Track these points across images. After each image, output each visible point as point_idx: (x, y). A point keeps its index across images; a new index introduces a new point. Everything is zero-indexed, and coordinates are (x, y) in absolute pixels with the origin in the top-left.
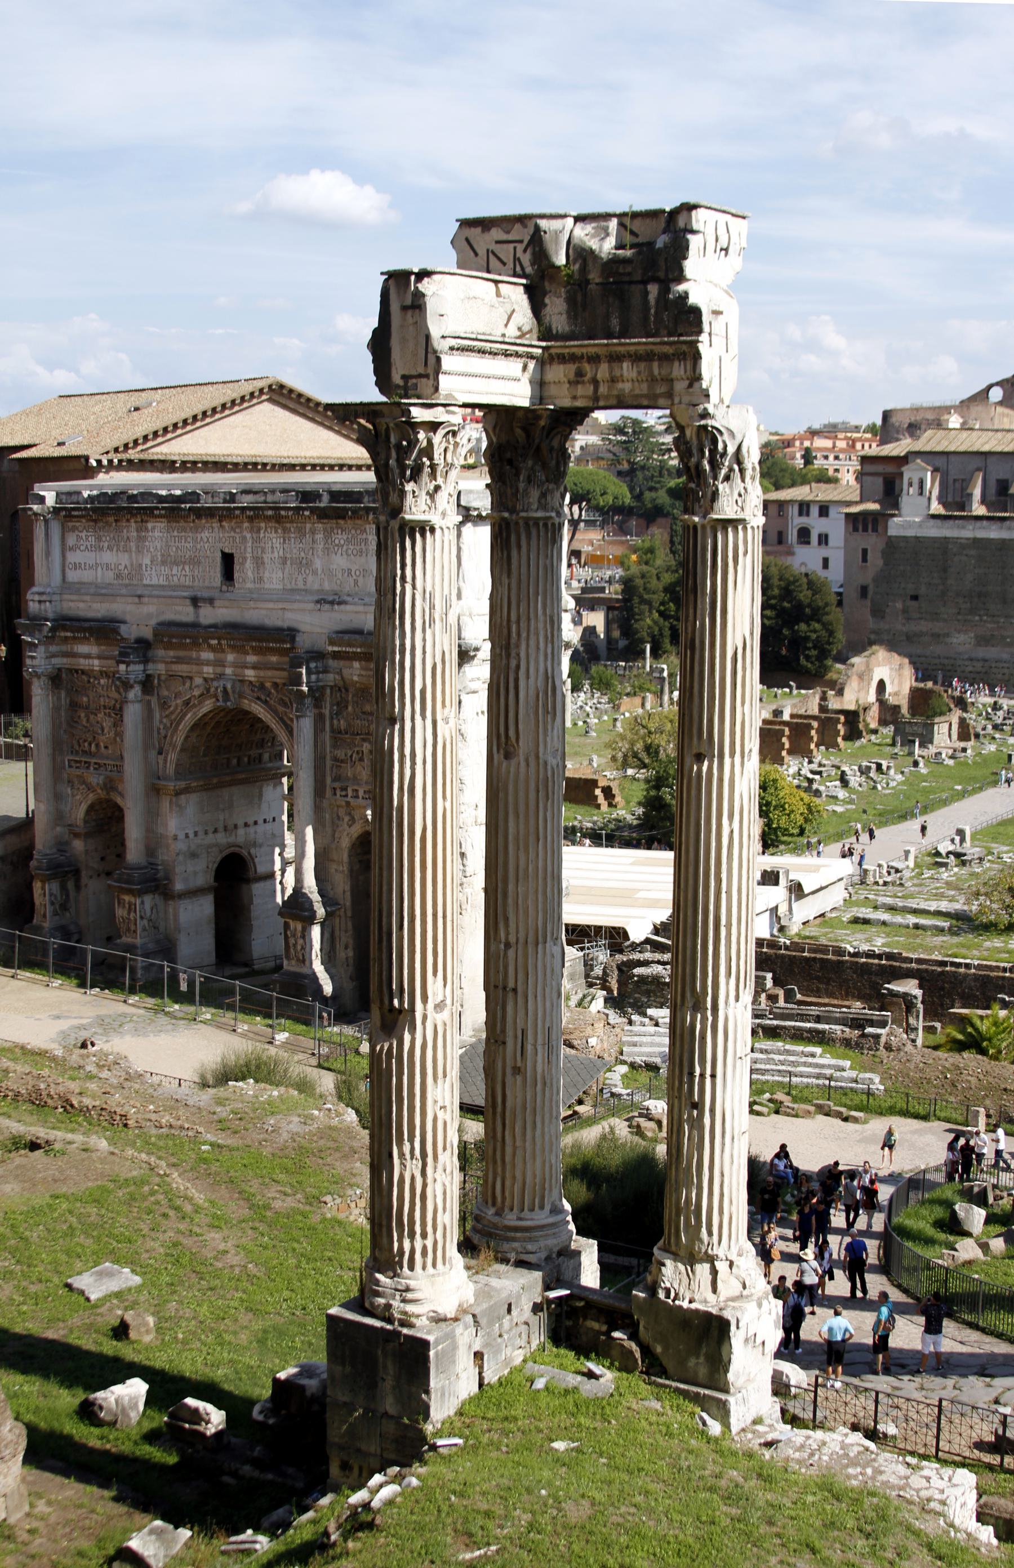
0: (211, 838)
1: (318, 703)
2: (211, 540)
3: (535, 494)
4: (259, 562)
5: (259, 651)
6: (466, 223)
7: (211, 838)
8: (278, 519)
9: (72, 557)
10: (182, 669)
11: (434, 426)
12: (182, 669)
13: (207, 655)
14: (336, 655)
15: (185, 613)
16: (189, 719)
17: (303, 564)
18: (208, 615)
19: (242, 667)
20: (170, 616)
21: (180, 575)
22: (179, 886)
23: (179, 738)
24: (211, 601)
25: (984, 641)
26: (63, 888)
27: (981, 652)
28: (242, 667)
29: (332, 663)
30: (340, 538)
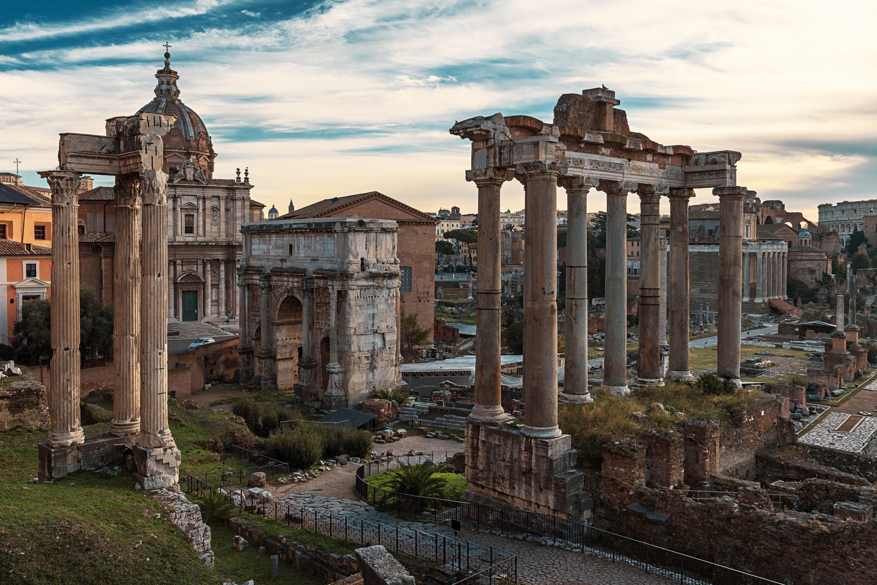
0: (292, 341)
1: (312, 292)
2: (287, 239)
3: (123, 200)
4: (298, 247)
5: (298, 277)
6: (108, 121)
7: (292, 341)
8: (303, 233)
9: (254, 247)
10: (279, 283)
11: (62, 178)
12: (279, 283)
13: (285, 279)
14: (317, 278)
15: (279, 264)
16: (281, 300)
17: (309, 247)
18: (286, 265)
19: (292, 283)
20: (276, 266)
21: (280, 252)
22: (279, 357)
23: (279, 306)
24: (285, 260)
25: (703, 291)
26: (248, 357)
27: (703, 296)
28: (292, 283)
29: (316, 281)
30: (318, 238)
